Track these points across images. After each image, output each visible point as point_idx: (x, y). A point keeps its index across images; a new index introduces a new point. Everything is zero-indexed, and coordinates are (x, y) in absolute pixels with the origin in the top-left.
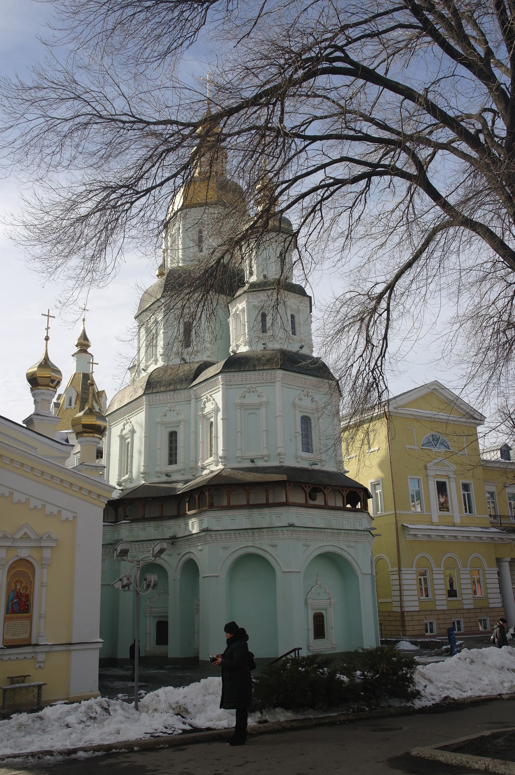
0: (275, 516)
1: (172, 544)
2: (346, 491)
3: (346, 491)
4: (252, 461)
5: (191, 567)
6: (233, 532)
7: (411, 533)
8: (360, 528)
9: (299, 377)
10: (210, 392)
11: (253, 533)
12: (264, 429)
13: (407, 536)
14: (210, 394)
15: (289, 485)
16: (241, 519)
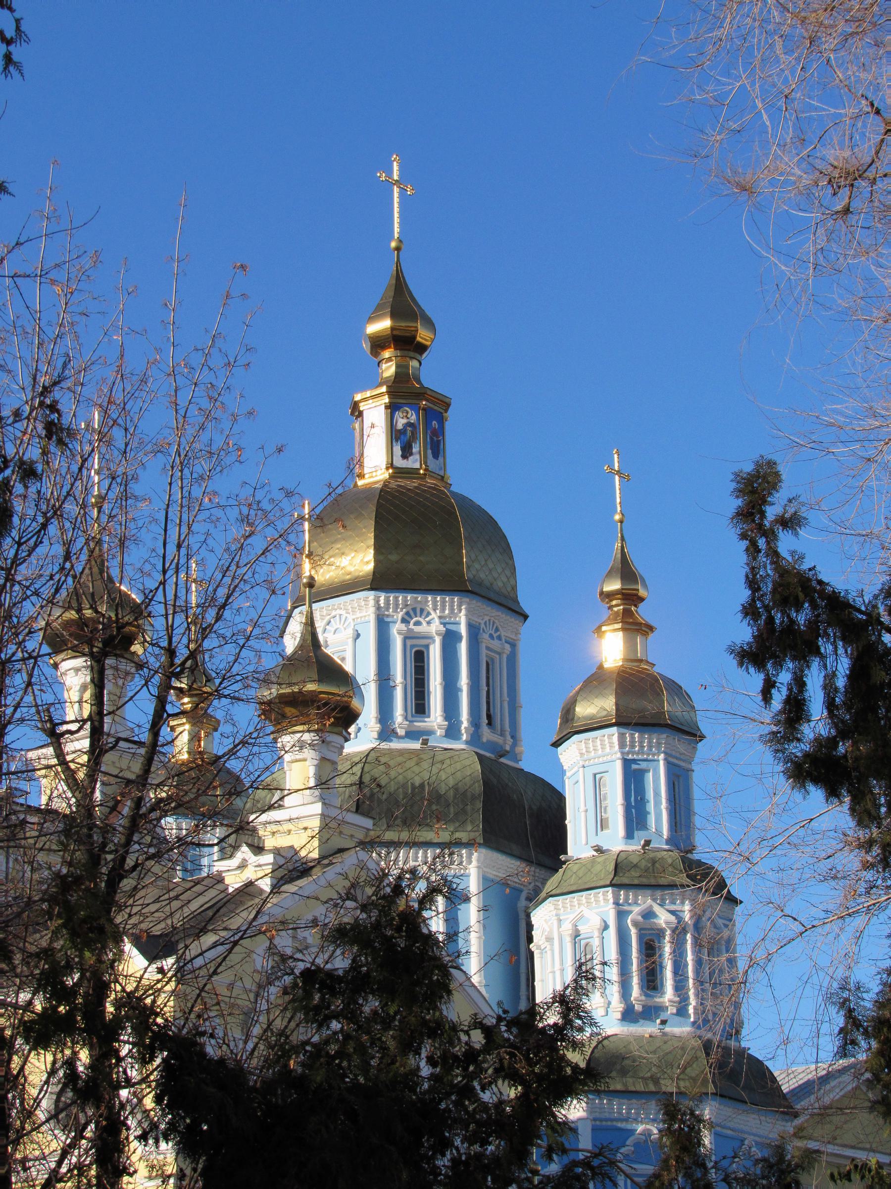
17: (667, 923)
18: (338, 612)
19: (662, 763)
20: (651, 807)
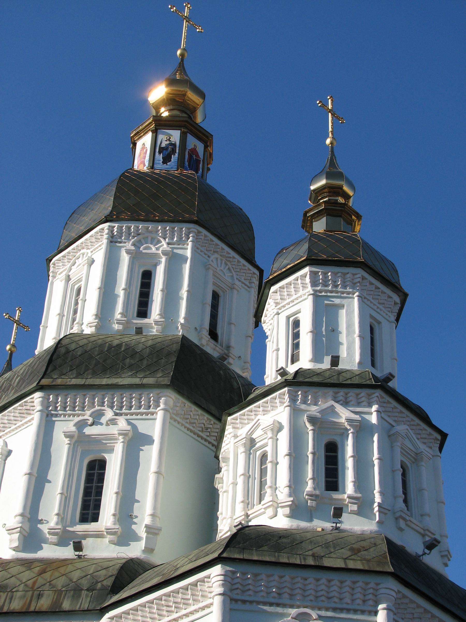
17: (349, 420)
18: (82, 251)
19: (356, 299)
20: (343, 338)
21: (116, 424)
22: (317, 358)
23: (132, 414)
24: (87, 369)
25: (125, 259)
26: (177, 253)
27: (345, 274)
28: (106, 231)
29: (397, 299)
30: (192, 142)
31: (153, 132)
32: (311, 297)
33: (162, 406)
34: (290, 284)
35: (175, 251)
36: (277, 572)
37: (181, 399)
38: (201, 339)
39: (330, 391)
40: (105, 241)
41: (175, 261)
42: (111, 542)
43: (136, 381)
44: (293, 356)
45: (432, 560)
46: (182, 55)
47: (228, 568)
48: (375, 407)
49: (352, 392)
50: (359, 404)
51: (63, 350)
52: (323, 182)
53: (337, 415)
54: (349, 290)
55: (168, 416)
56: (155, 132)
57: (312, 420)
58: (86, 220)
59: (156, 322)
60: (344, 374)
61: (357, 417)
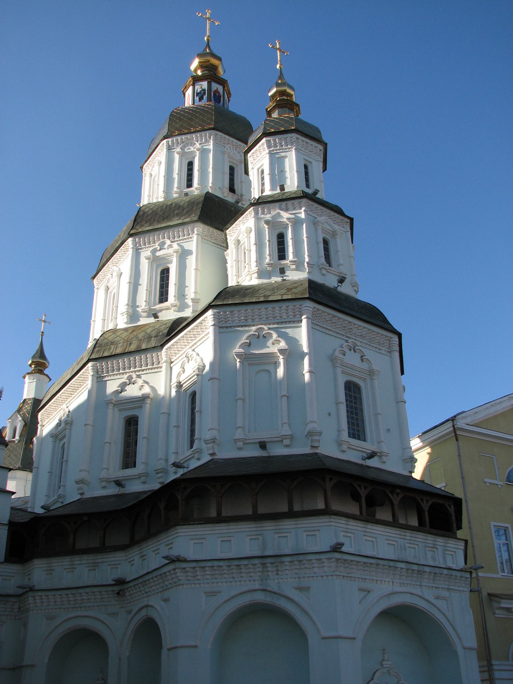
0: (305, 534)
1: (118, 593)
2: (427, 501)
3: (427, 501)
4: (263, 445)
5: (149, 633)
6: (227, 563)
7: (503, 605)
8: (454, 567)
9: (339, 318)
10: (193, 345)
11: (263, 564)
12: (285, 393)
13: (497, 611)
14: (193, 348)
15: (331, 479)
16: (240, 539)
17: (288, 219)
19: (294, 151)
20: (288, 175)
21: (172, 247)
22: (273, 188)
23: (180, 240)
24: (154, 220)
25: (177, 157)
26: (205, 149)
27: (286, 138)
28: (165, 144)
29: (321, 147)
30: (215, 86)
31: (192, 85)
32: (268, 155)
33: (196, 232)
34: (257, 150)
35: (204, 147)
36: (243, 308)
37: (207, 227)
38: (223, 193)
39: (277, 204)
40: (165, 150)
41: (204, 152)
42: (174, 311)
43: (180, 221)
44: (262, 190)
45: (345, 289)
46: (208, 40)
47: (216, 311)
48: (303, 209)
49: (290, 203)
50: (294, 209)
51: (141, 213)
52: (274, 90)
53: (282, 217)
54: (289, 147)
55: (200, 237)
56: (194, 85)
57: (267, 222)
58: (157, 141)
59: (196, 189)
60: (285, 194)
61: (293, 216)
